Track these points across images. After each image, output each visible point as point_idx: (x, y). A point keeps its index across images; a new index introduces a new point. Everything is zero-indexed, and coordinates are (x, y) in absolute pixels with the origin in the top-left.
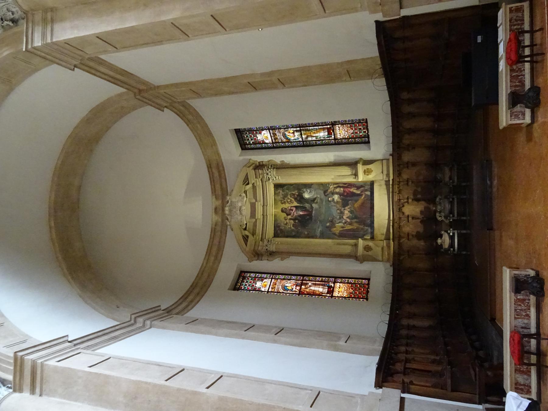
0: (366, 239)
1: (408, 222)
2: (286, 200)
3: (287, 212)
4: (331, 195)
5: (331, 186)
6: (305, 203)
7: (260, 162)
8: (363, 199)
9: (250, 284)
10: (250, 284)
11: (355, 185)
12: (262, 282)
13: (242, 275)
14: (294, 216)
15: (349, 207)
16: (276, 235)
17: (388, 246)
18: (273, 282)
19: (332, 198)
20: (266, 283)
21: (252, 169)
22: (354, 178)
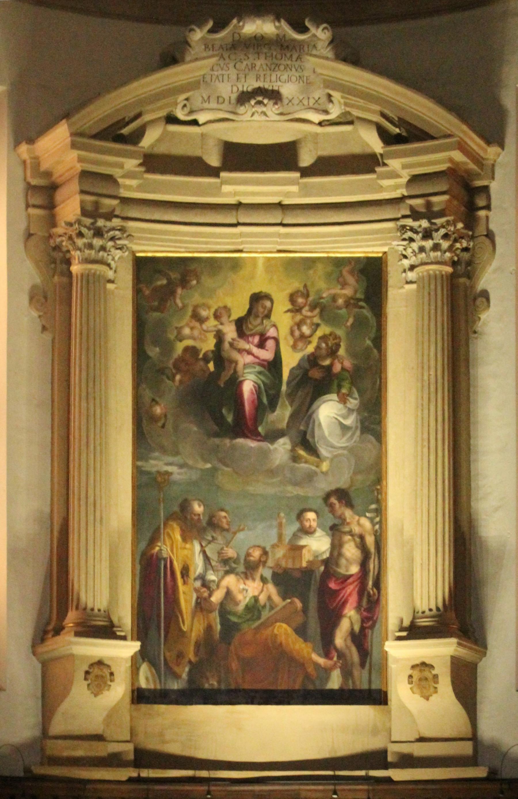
2: (309, 314)
3: (251, 319)
4: (330, 520)
5: (371, 520)
6: (291, 407)
8: (311, 659)
11: (372, 627)
14: (235, 355)
15: (276, 598)
19: (314, 524)
22: (402, 621)
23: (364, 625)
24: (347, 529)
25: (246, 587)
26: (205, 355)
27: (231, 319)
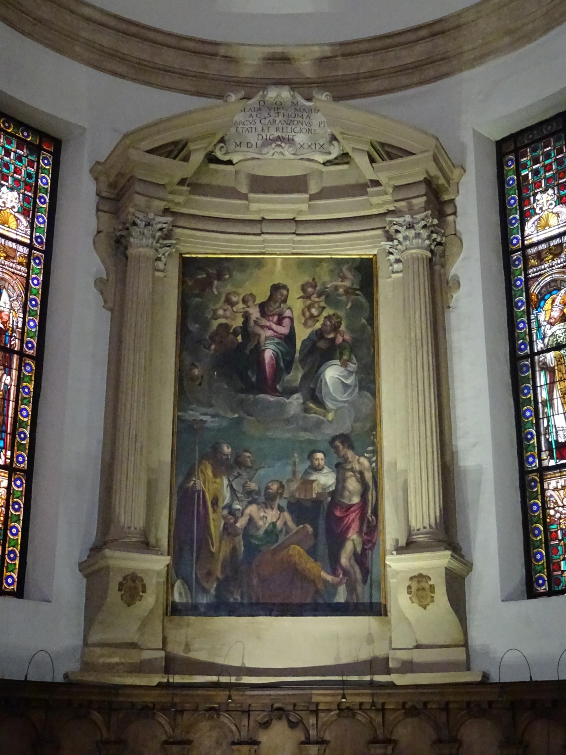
0: (169, 586)
1: (234, 743)
2: (317, 299)
3: (272, 303)
5: (369, 459)
6: (303, 369)
7: (455, 207)
8: (320, 576)
9: (12, 167)
10: (12, 167)
11: (372, 549)
12: (18, 212)
14: (259, 330)
15: (291, 524)
18: (15, 250)
19: (322, 463)
20: (13, 224)
21: (427, 172)
23: (365, 547)
24: (349, 467)
25: (266, 515)
26: (235, 330)
27: (256, 303)
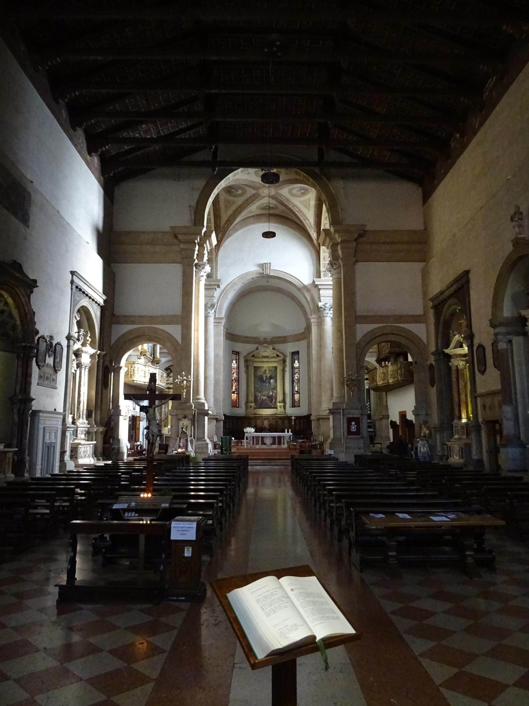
13: (237, 353)
16: (255, 367)
17: (251, 415)
